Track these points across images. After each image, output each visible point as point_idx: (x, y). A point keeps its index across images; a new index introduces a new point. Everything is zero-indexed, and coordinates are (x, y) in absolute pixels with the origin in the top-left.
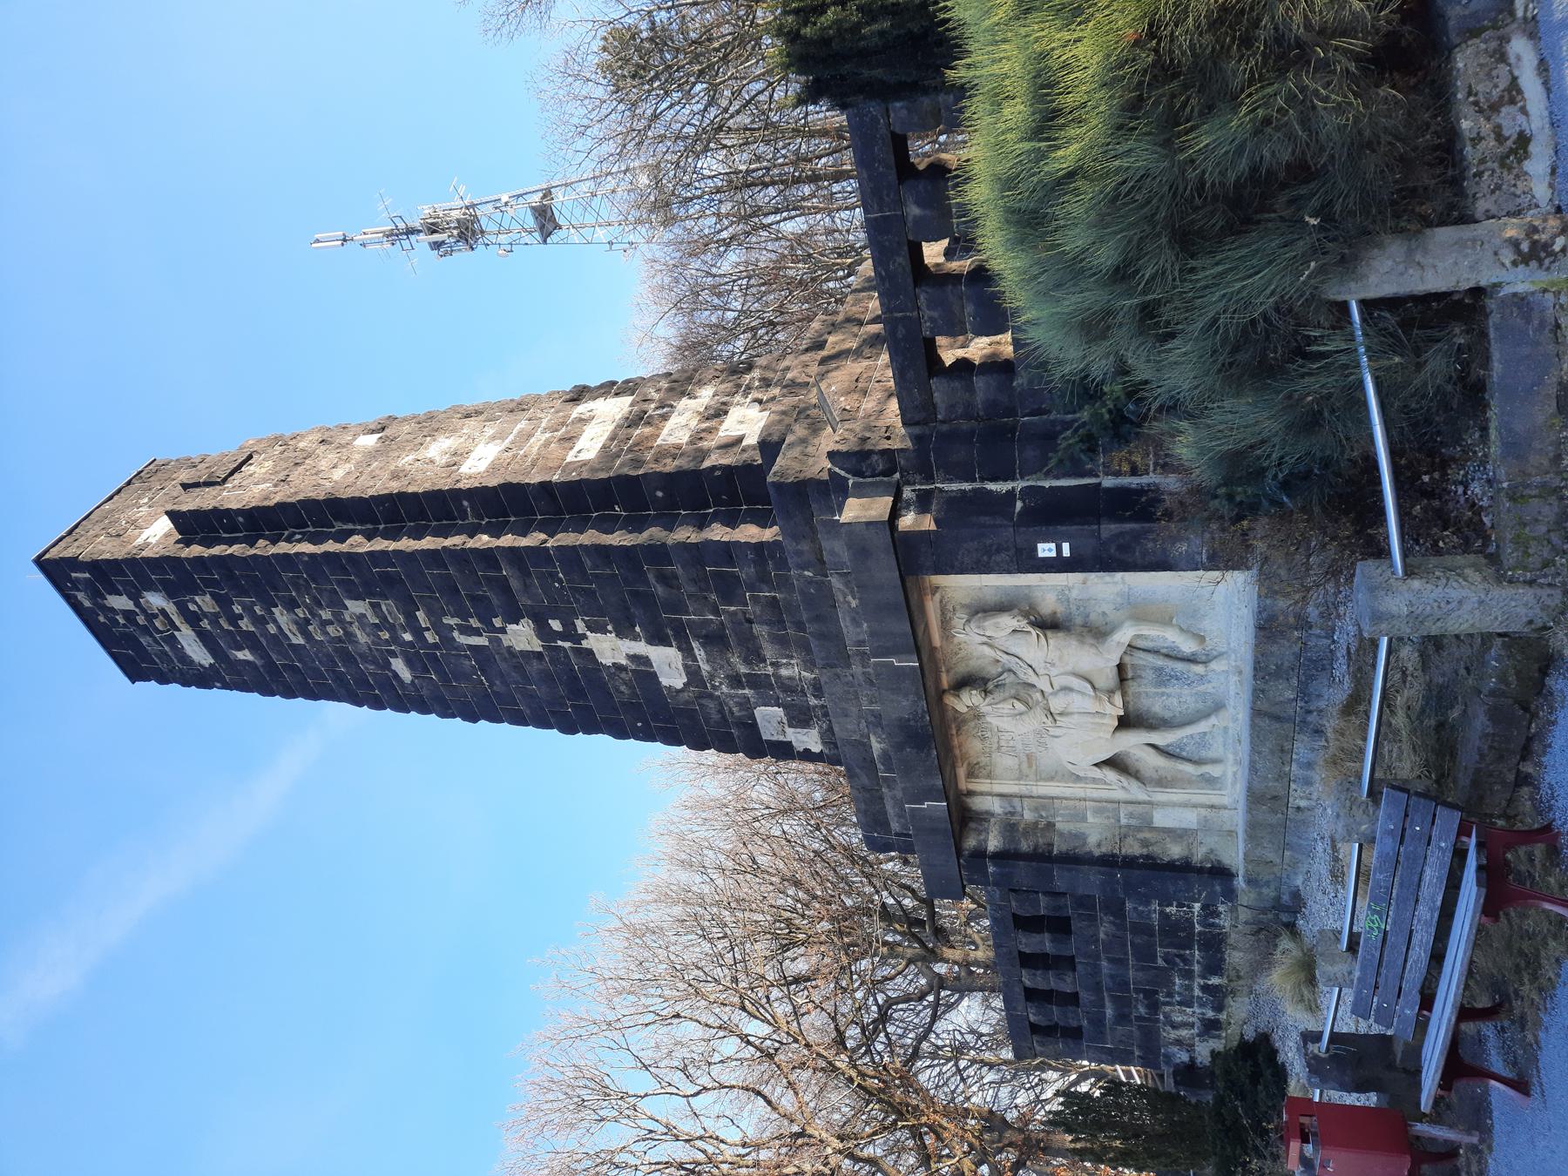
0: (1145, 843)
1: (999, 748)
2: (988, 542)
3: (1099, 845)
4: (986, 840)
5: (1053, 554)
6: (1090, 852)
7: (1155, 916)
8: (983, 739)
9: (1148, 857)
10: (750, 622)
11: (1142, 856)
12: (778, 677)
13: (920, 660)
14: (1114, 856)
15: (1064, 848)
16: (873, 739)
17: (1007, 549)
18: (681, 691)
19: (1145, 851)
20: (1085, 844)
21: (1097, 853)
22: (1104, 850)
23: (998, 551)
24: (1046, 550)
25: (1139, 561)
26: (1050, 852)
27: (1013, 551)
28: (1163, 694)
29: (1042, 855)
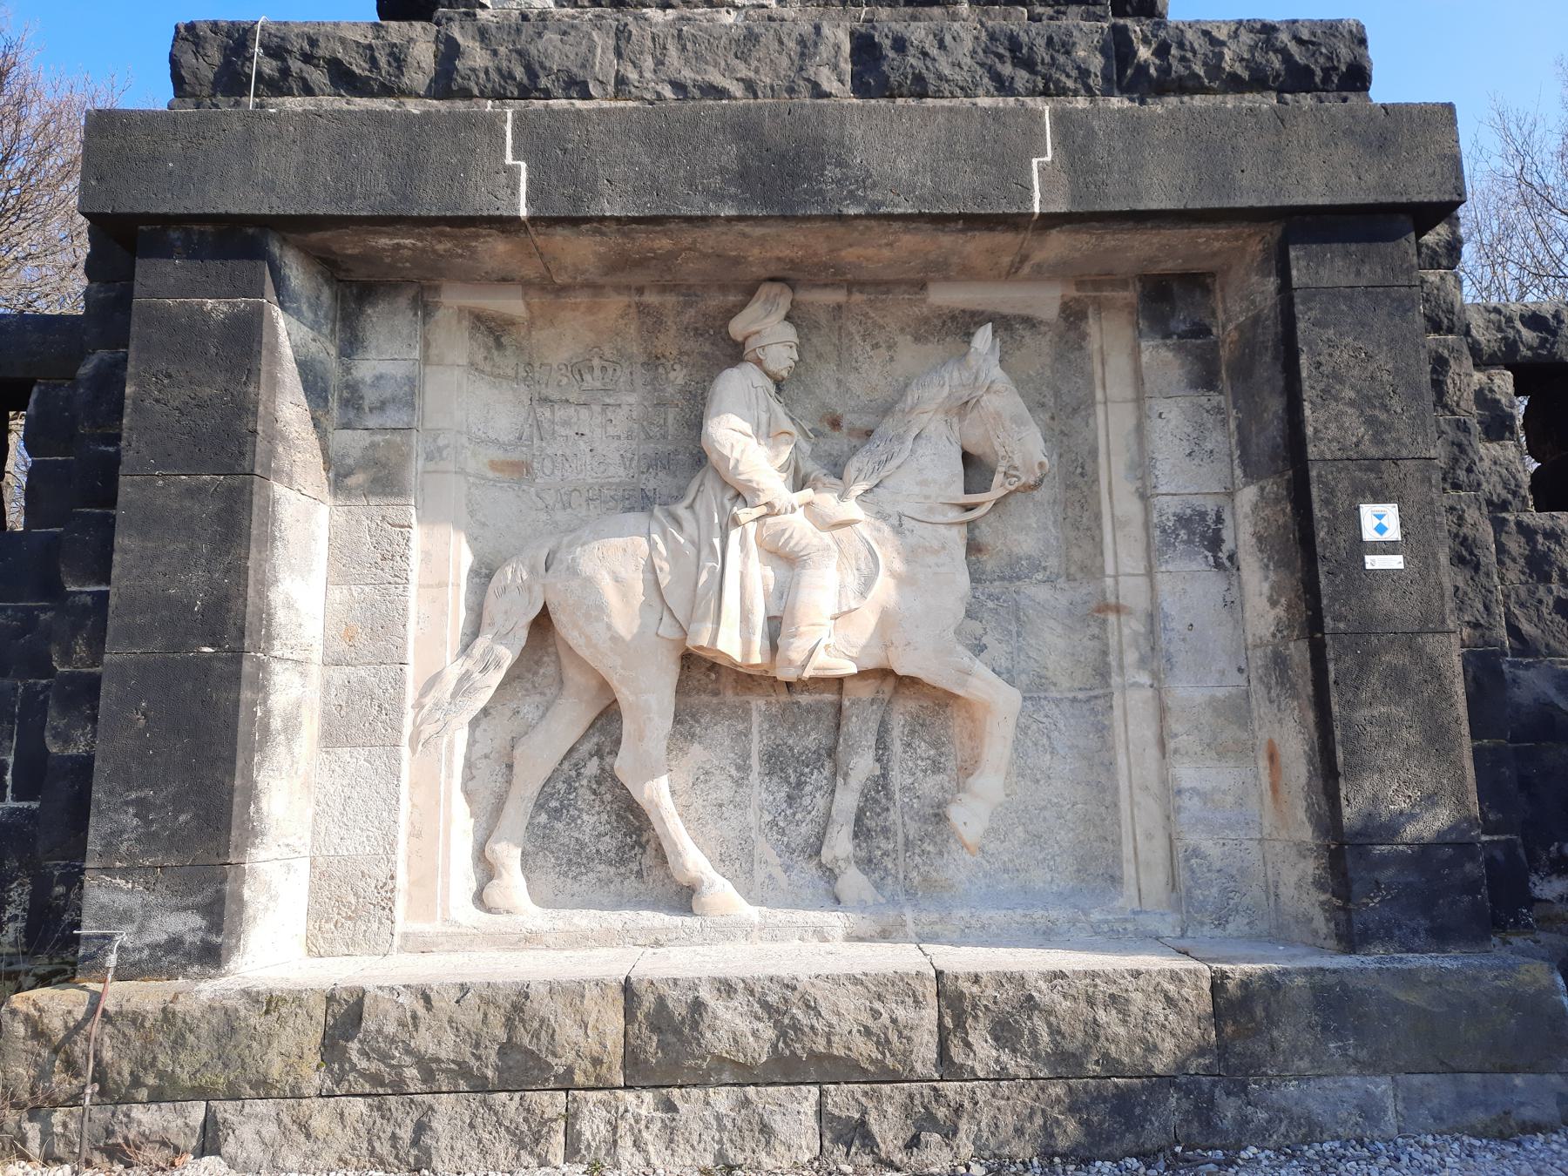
0: (292, 725)
1: (545, 400)
2: (1396, 404)
3: (289, 606)
5: (1369, 534)
8: (578, 369)
9: (266, 729)
11: (268, 713)
13: (1050, 221)
14: (269, 638)
17: (1378, 440)
19: (276, 723)
22: (281, 616)
23: (1371, 422)
24: (1380, 520)
27: (1374, 452)
28: (744, 768)
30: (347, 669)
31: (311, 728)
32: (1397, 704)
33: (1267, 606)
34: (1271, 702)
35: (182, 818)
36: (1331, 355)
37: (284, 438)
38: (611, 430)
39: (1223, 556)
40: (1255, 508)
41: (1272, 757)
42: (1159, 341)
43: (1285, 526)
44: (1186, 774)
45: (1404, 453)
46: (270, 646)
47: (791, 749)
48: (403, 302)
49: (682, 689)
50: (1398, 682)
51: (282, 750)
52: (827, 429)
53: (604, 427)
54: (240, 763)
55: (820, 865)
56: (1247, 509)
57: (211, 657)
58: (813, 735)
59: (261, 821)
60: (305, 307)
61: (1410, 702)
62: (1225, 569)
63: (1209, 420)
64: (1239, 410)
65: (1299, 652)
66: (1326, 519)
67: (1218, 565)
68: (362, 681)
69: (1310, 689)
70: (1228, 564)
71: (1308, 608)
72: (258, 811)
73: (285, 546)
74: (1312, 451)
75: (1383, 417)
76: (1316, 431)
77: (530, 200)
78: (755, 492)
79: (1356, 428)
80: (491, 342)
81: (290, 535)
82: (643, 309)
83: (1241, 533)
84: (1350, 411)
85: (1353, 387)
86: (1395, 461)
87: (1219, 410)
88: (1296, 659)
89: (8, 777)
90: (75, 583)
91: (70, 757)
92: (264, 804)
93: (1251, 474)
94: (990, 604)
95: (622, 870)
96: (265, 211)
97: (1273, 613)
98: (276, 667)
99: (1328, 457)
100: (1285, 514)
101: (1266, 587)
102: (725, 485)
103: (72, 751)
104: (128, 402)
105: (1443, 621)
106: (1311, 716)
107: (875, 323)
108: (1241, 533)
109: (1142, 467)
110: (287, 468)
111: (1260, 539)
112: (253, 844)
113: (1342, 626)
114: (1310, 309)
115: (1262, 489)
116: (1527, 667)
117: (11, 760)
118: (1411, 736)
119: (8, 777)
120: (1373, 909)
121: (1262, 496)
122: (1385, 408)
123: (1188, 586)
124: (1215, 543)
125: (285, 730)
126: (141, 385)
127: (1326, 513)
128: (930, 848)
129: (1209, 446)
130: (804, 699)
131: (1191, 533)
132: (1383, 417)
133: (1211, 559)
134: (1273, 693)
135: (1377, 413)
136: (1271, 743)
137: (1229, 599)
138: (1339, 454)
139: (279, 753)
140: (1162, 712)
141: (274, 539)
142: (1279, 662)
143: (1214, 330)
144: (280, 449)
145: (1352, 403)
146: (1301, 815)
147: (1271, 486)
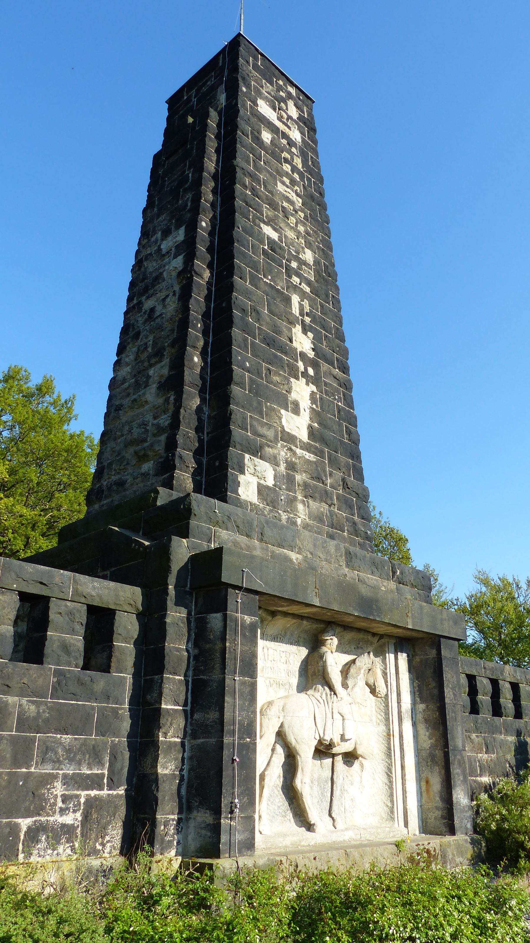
7: (47, 769)
10: (330, 506)
18: (281, 422)
27: (454, 702)
33: (428, 739)
34: (428, 766)
35: (245, 800)
40: (424, 711)
41: (427, 782)
43: (436, 718)
56: (421, 710)
64: (419, 681)
65: (439, 754)
69: (443, 764)
71: (443, 742)
88: (438, 755)
90: (166, 704)
91: (165, 774)
93: (422, 701)
95: (285, 819)
97: (429, 742)
100: (436, 715)
101: (427, 734)
103: (166, 772)
104: (227, 649)
106: (443, 772)
111: (426, 721)
115: (427, 706)
117: (106, 773)
118: (461, 778)
121: (427, 708)
122: (455, 690)
126: (230, 643)
134: (429, 764)
136: (427, 778)
142: (432, 757)
145: (451, 689)
146: (438, 798)
147: (431, 706)
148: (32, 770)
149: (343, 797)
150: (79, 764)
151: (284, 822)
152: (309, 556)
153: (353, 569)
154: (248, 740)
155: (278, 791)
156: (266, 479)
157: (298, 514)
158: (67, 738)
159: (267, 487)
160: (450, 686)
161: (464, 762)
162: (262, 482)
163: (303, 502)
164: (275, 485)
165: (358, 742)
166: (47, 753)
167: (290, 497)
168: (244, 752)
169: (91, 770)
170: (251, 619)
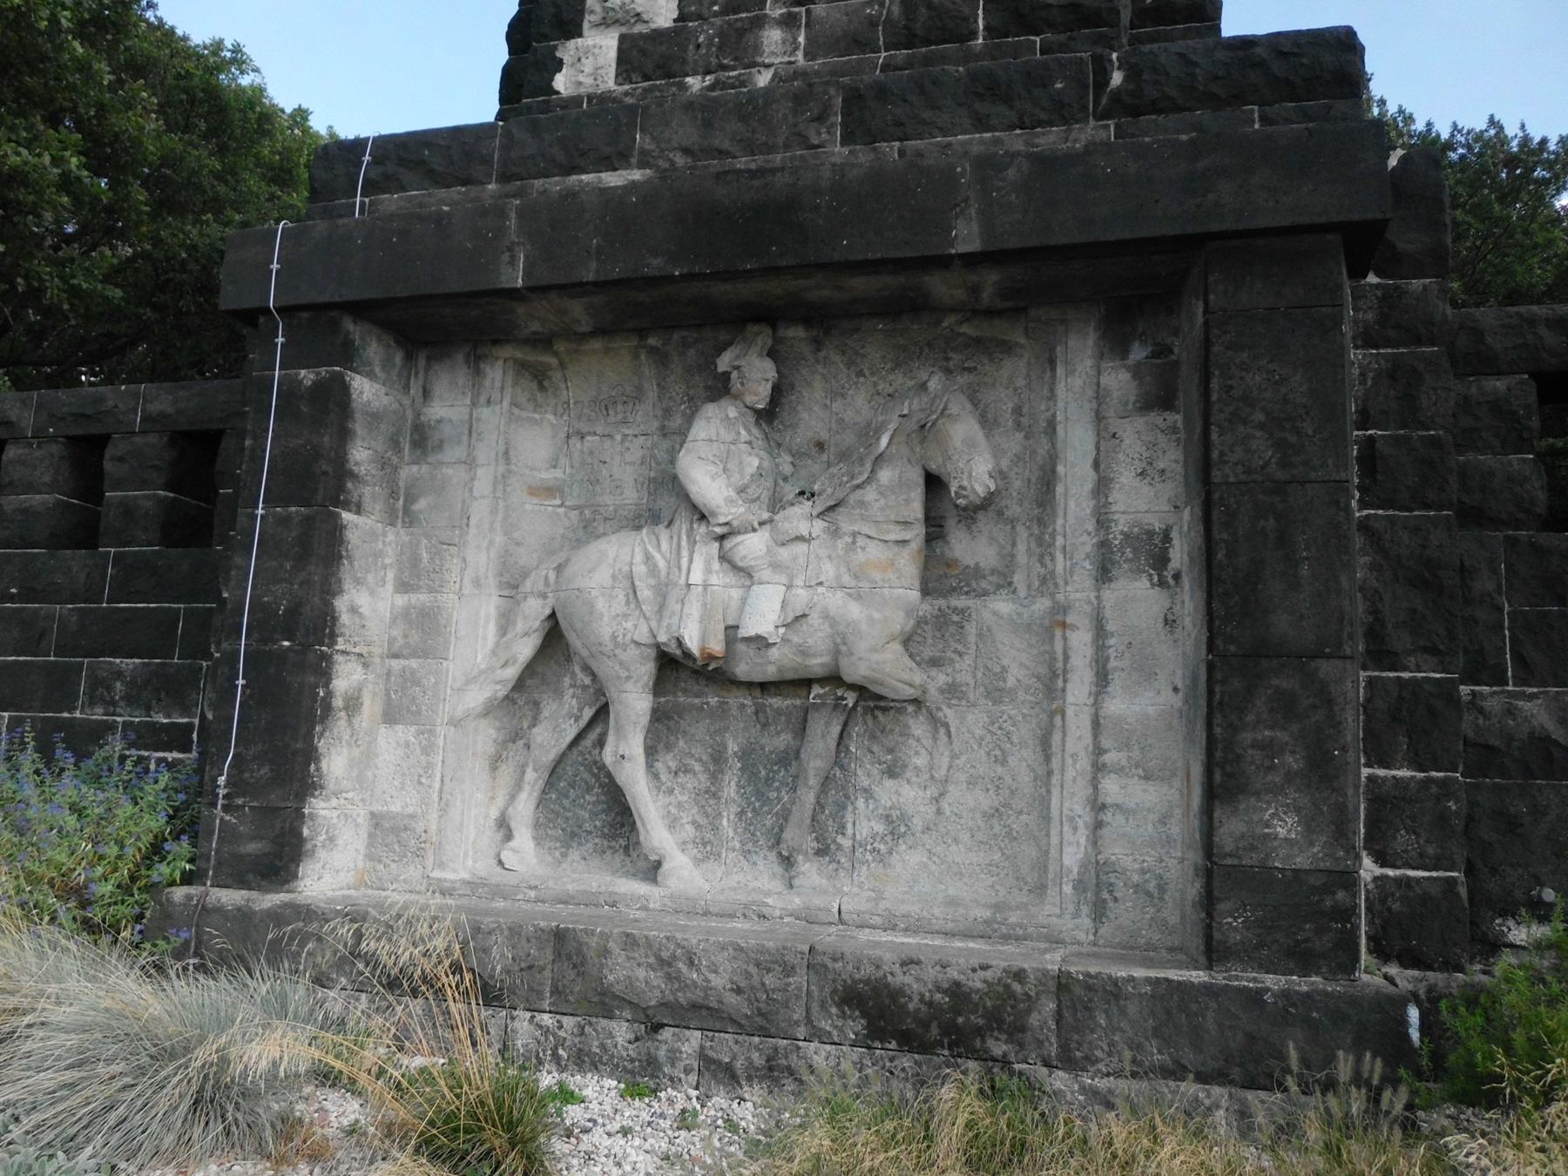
0: (353, 704)
3: (354, 610)
4: (371, 375)
6: (341, 591)
7: (98, 715)
9: (327, 708)
11: (329, 694)
12: (759, 22)
14: (333, 637)
15: (353, 537)
16: (636, 175)
19: (338, 702)
20: (358, 582)
21: (341, 604)
22: (345, 618)
25: (1247, 737)
26: (346, 505)
27: (1282, 475)
29: (341, 488)
30: (402, 661)
31: (370, 707)
32: (1283, 729)
36: (1242, 378)
37: (354, 476)
38: (628, 457)
39: (1168, 575)
42: (1118, 363)
44: (1111, 787)
45: (1313, 475)
46: (333, 642)
47: (763, 748)
48: (460, 357)
49: (659, 686)
50: (1286, 707)
51: (342, 723)
52: (814, 450)
53: (622, 454)
54: (303, 730)
55: (780, 854)
57: (289, 649)
58: (783, 736)
59: (321, 777)
60: (377, 369)
61: (1295, 727)
62: (1169, 587)
63: (1161, 438)
66: (1225, 541)
67: (1162, 583)
68: (413, 672)
70: (1171, 582)
72: (318, 769)
73: (351, 563)
74: (1217, 475)
75: (1293, 439)
76: (1222, 454)
77: (527, 274)
78: (714, 514)
79: (1263, 450)
80: (535, 385)
81: (357, 554)
82: (653, 351)
83: (1179, 555)
84: (1259, 434)
85: (1264, 410)
86: (1302, 483)
87: (1174, 430)
89: (195, 736)
92: (324, 764)
94: (955, 618)
96: (337, 299)
98: (339, 658)
99: (1232, 479)
102: (694, 507)
105: (1340, 645)
107: (856, 353)
108: (1179, 555)
109: (1102, 486)
110: (355, 499)
112: (313, 796)
113: (1232, 648)
114: (1225, 333)
116: (1531, 697)
118: (1294, 762)
119: (195, 736)
120: (1235, 929)
123: (1137, 600)
124: (1160, 560)
125: (346, 708)
127: (1225, 536)
128: (882, 847)
129: (1162, 465)
130: (776, 702)
131: (1135, 550)
132: (1293, 439)
133: (1156, 578)
135: (1287, 435)
137: (1170, 617)
138: (1243, 477)
139: (340, 724)
140: (1096, 724)
141: (341, 557)
143: (1176, 350)
144: (349, 485)
145: (1261, 426)
148: (78, 715)
149: (850, 808)
150: (148, 709)
151: (609, 853)
152: (680, 160)
153: (871, 138)
154: (286, 643)
155: (594, 775)
156: (645, 17)
157: (759, 60)
158: (128, 664)
159: (658, 34)
160: (1259, 417)
161: (1329, 702)
162: (639, 28)
163: (789, 22)
164: (682, 18)
165: (844, 648)
166: (99, 691)
167: (739, 24)
168: (272, 670)
169: (169, 716)
170: (318, 374)
